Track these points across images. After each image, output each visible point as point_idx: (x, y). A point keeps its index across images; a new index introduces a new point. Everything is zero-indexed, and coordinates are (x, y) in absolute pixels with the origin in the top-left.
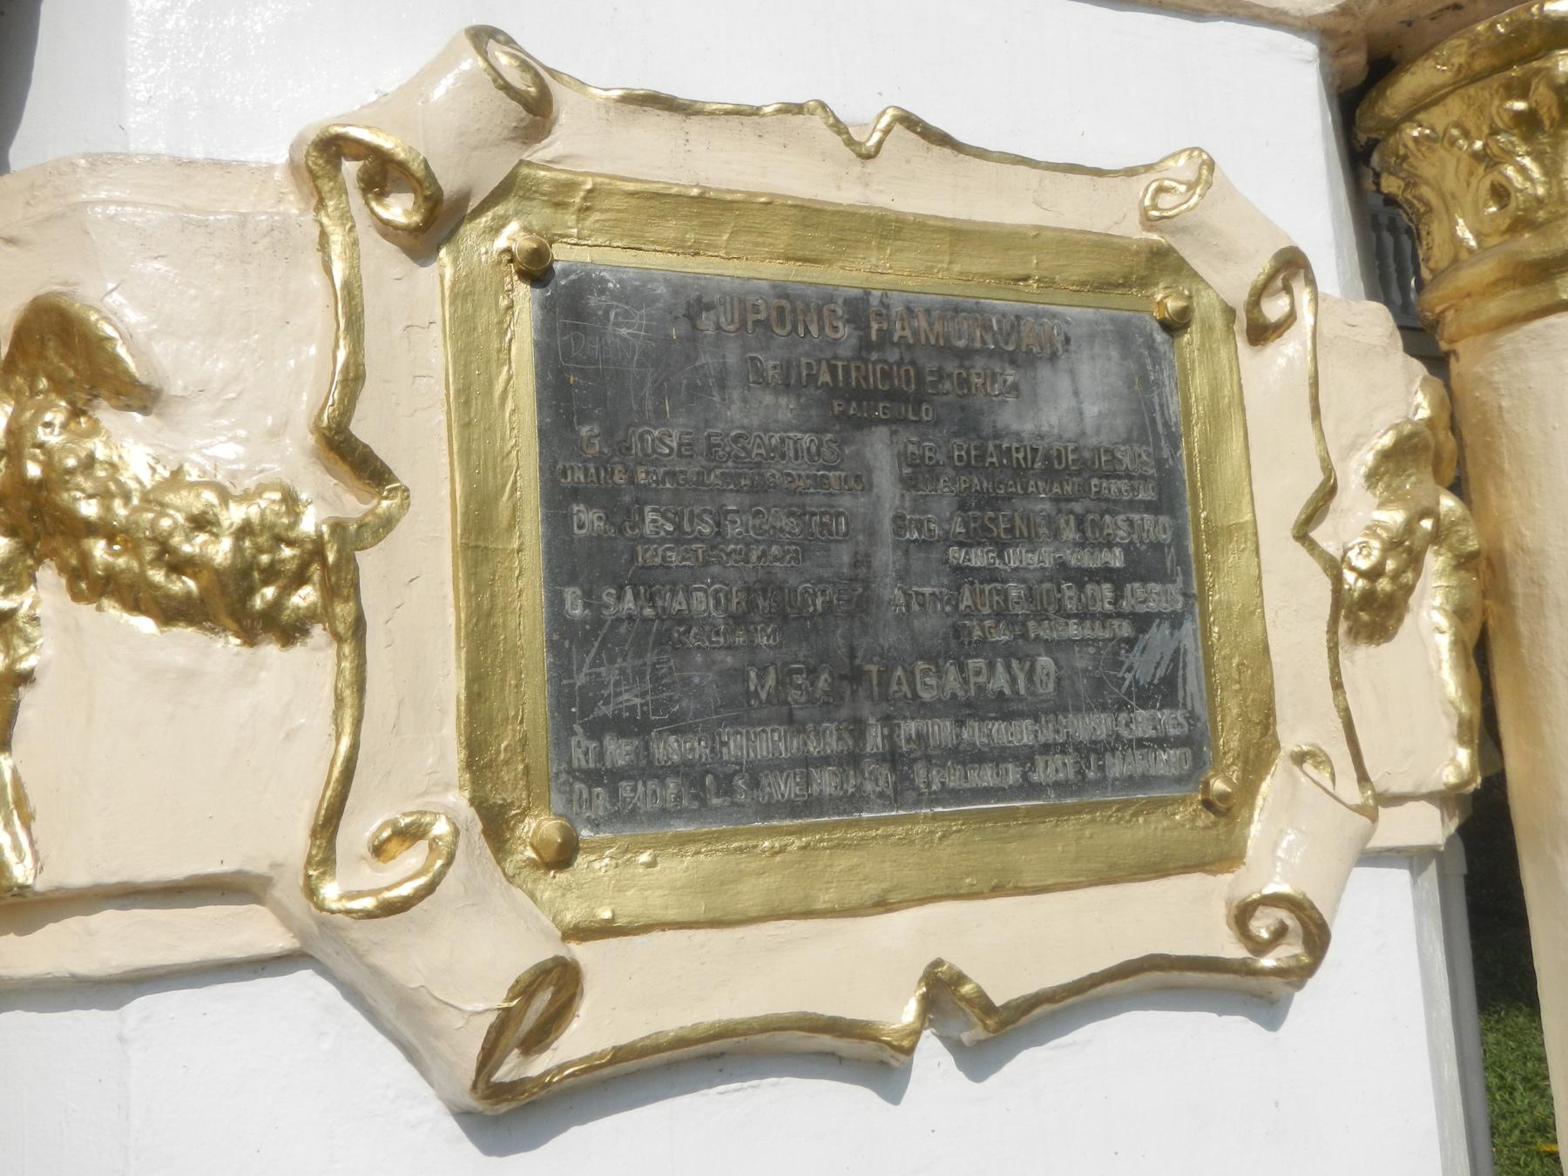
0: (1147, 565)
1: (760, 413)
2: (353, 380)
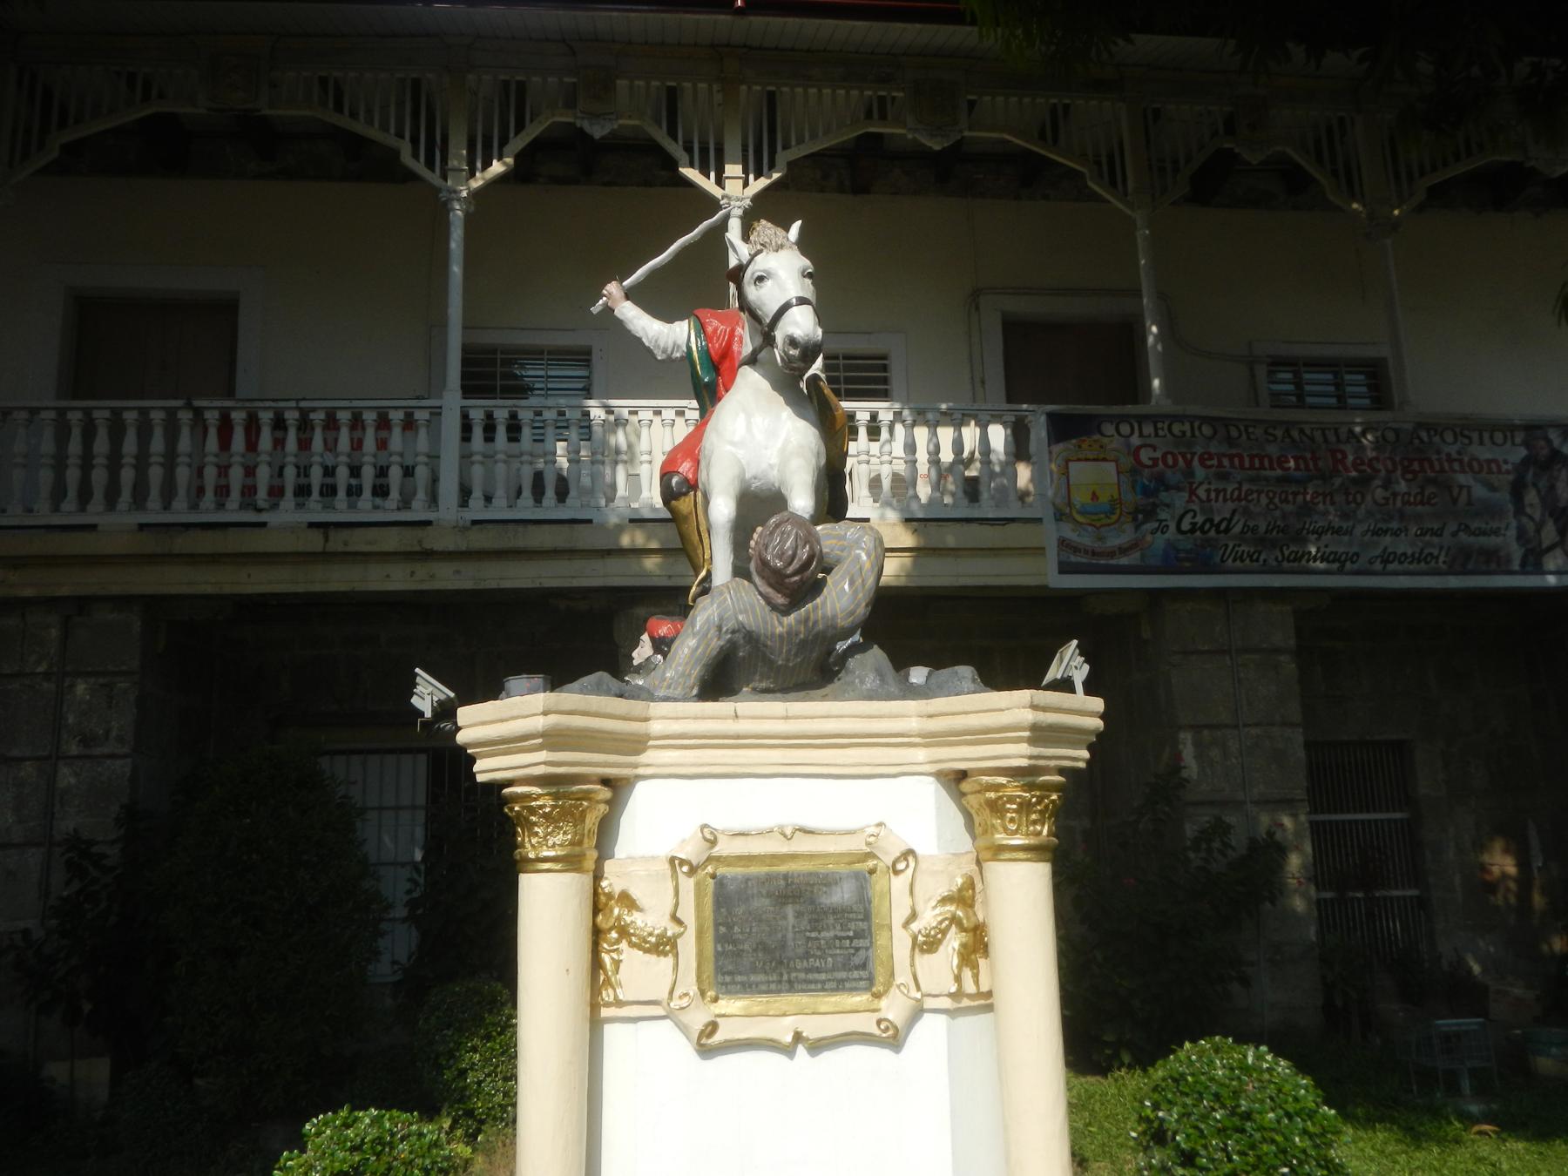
0: (859, 935)
1: (762, 904)
2: (677, 905)
